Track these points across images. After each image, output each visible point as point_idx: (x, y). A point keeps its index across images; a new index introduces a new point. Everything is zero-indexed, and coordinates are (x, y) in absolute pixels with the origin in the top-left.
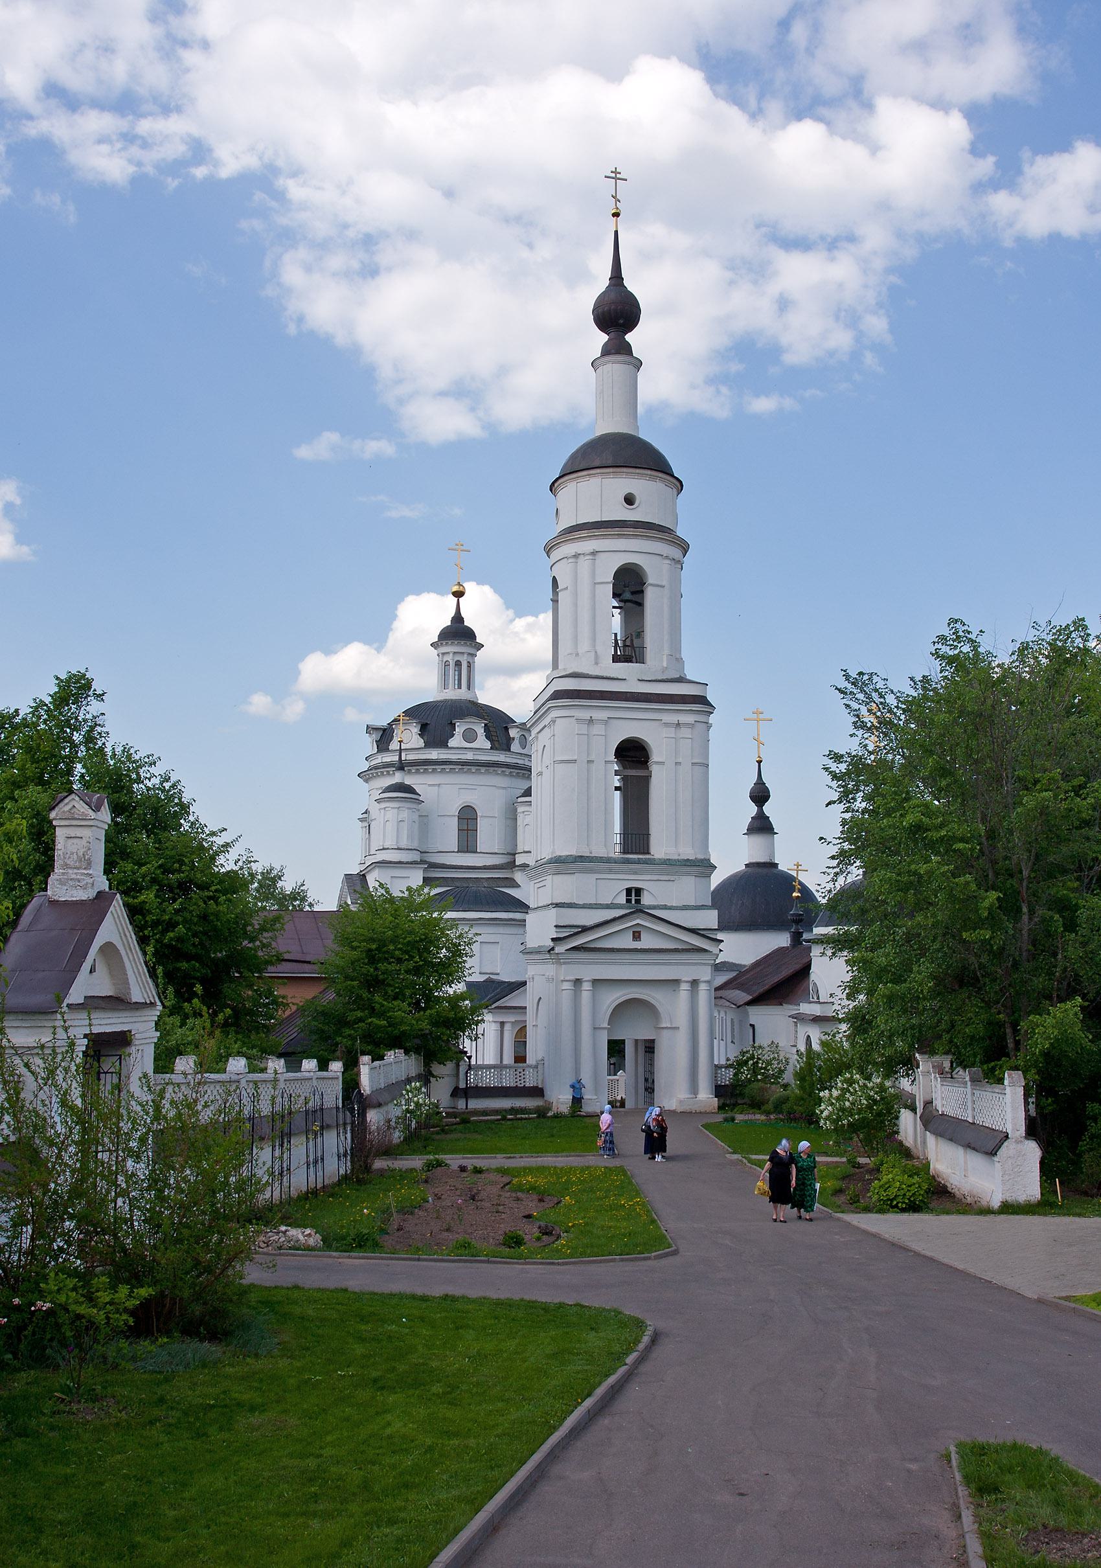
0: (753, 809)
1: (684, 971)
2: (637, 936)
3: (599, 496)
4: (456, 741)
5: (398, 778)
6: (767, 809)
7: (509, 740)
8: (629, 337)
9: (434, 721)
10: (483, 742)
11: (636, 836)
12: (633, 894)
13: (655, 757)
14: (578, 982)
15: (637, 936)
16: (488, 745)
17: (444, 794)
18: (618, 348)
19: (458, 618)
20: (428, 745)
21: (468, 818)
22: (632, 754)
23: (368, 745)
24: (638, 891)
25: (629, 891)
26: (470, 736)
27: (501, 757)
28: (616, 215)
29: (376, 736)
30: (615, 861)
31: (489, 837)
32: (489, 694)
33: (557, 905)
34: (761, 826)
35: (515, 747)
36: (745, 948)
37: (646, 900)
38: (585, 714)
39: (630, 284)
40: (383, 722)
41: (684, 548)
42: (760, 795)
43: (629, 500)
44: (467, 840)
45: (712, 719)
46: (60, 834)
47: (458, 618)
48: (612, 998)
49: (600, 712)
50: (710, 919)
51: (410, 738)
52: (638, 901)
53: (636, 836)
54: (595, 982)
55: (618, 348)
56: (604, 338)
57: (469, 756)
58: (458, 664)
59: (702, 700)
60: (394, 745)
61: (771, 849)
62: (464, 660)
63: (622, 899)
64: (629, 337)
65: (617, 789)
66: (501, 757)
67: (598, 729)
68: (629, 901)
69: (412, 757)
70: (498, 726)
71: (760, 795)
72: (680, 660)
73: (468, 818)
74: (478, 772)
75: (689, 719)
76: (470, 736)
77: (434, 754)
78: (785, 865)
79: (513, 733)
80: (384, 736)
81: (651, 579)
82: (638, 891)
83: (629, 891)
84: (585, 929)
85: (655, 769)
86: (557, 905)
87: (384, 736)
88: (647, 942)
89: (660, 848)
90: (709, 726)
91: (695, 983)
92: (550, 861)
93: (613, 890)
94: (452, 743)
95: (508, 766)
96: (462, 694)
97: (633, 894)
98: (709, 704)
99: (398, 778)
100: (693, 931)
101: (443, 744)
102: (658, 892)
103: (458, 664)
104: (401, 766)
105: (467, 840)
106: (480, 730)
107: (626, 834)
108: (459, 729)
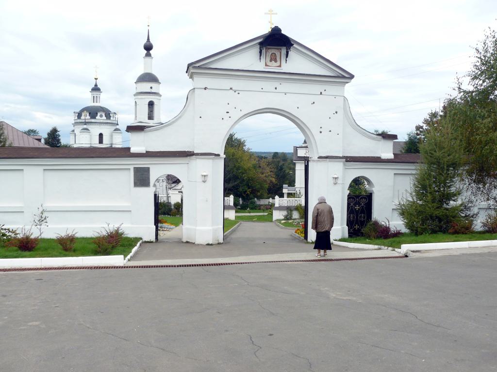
3: (146, 87)
5: (85, 126)
7: (110, 117)
10: (104, 118)
16: (106, 118)
17: (95, 130)
18: (148, 55)
19: (96, 85)
21: (101, 135)
26: (101, 116)
27: (109, 121)
29: (77, 115)
35: (112, 118)
41: (160, 96)
43: (151, 88)
44: (101, 141)
47: (96, 85)
51: (86, 116)
55: (148, 55)
56: (146, 52)
57: (101, 121)
58: (97, 97)
60: (83, 117)
64: (151, 52)
66: (109, 121)
69: (87, 121)
70: (108, 114)
73: (101, 135)
76: (101, 116)
77: (93, 120)
79: (111, 115)
81: (155, 103)
87: (79, 115)
94: (97, 118)
95: (110, 123)
103: (97, 97)
104: (86, 123)
105: (101, 141)
106: (104, 115)
108: (99, 114)
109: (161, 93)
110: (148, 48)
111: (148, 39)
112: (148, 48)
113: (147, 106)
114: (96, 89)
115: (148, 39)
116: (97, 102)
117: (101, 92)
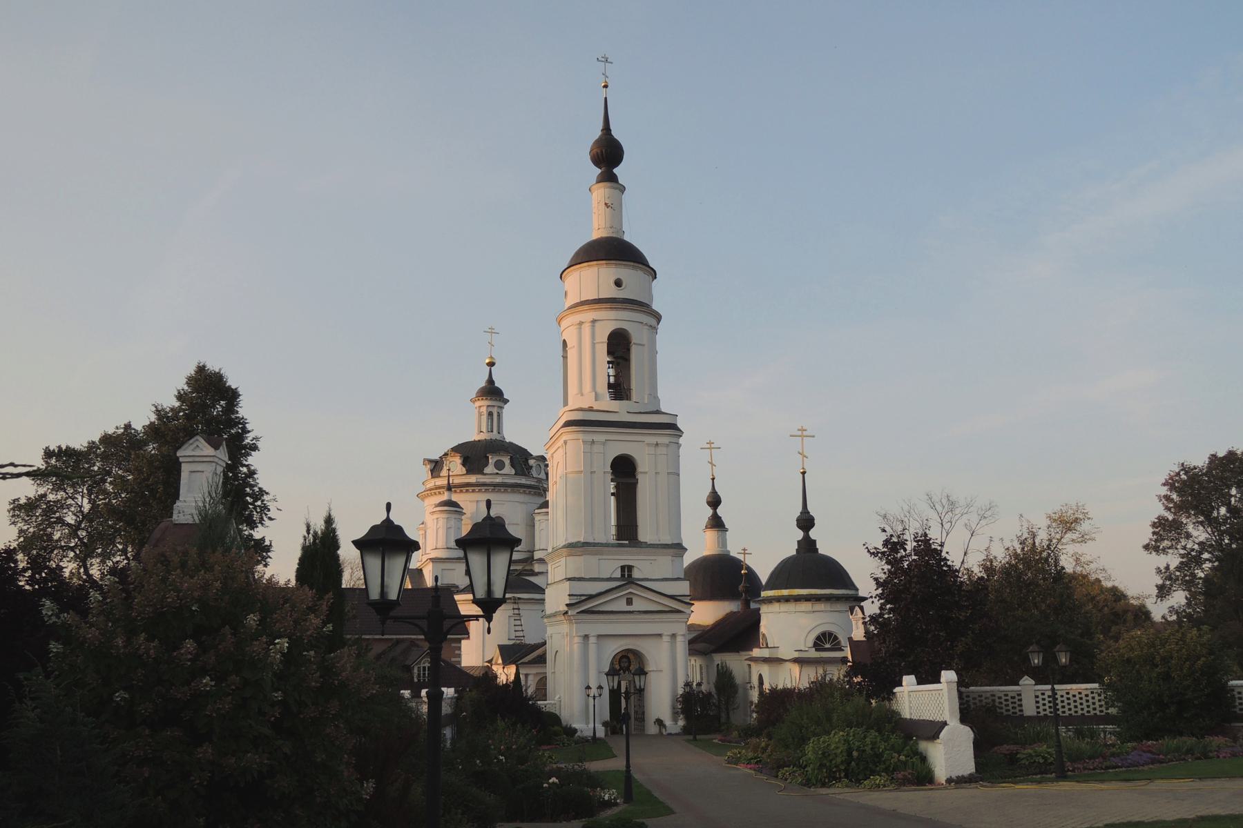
0: (710, 511)
1: (666, 626)
2: (629, 602)
3: (596, 279)
4: (490, 469)
6: (720, 511)
8: (616, 171)
9: (472, 456)
10: (508, 469)
11: (627, 529)
12: (627, 570)
13: (640, 469)
14: (586, 637)
15: (629, 602)
16: (513, 472)
18: (609, 177)
19: (491, 381)
20: (469, 472)
22: (624, 469)
23: (425, 471)
24: (630, 568)
25: (623, 568)
26: (500, 465)
27: (523, 481)
28: (606, 86)
30: (613, 546)
32: (513, 433)
33: (569, 579)
34: (716, 523)
35: (534, 472)
36: (706, 613)
37: (636, 574)
38: (589, 437)
39: (616, 133)
40: (437, 457)
41: (658, 317)
42: (715, 501)
43: (618, 283)
45: (681, 440)
46: (185, 469)
47: (491, 381)
48: (614, 648)
49: (600, 436)
50: (684, 588)
51: (455, 465)
52: (630, 576)
53: (627, 529)
54: (599, 636)
57: (498, 480)
59: (673, 426)
60: (444, 473)
61: (723, 543)
62: (495, 411)
63: (618, 574)
64: (616, 171)
65: (613, 494)
66: (523, 481)
67: (597, 448)
68: (623, 575)
69: (457, 481)
70: (520, 458)
71: (715, 501)
72: (656, 399)
74: (505, 491)
75: (666, 440)
76: (500, 465)
77: (472, 479)
78: (734, 552)
79: (531, 462)
80: (436, 466)
81: (634, 340)
82: (630, 568)
83: (623, 568)
84: (591, 597)
85: (639, 477)
86: (569, 579)
87: (436, 466)
88: (638, 605)
89: (645, 535)
90: (679, 445)
91: (674, 636)
92: (564, 547)
93: (610, 566)
94: (487, 470)
96: (494, 435)
97: (627, 570)
98: (679, 430)
100: (672, 597)
101: (481, 472)
102: (646, 567)
103: (490, 414)
104: (449, 488)
106: (507, 461)
107: (619, 526)
108: (492, 460)
109: (655, 307)
110: (608, 155)
111: (607, 128)
112: (608, 155)
113: (602, 349)
114: (492, 392)
115: (607, 128)
117: (506, 401)
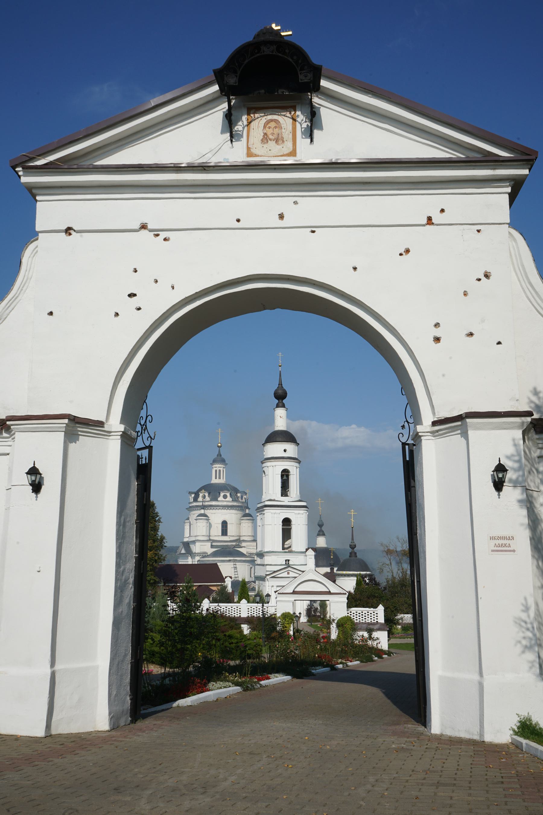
4: (221, 498)
10: (229, 498)
16: (231, 500)
21: (224, 524)
26: (225, 497)
27: (235, 504)
31: (231, 530)
40: (195, 490)
44: (224, 532)
57: (225, 504)
60: (200, 499)
66: (235, 504)
73: (224, 524)
76: (225, 497)
77: (214, 503)
94: (219, 499)
99: (202, 511)
105: (224, 532)
106: (228, 495)
108: (222, 494)
116: (220, 478)
